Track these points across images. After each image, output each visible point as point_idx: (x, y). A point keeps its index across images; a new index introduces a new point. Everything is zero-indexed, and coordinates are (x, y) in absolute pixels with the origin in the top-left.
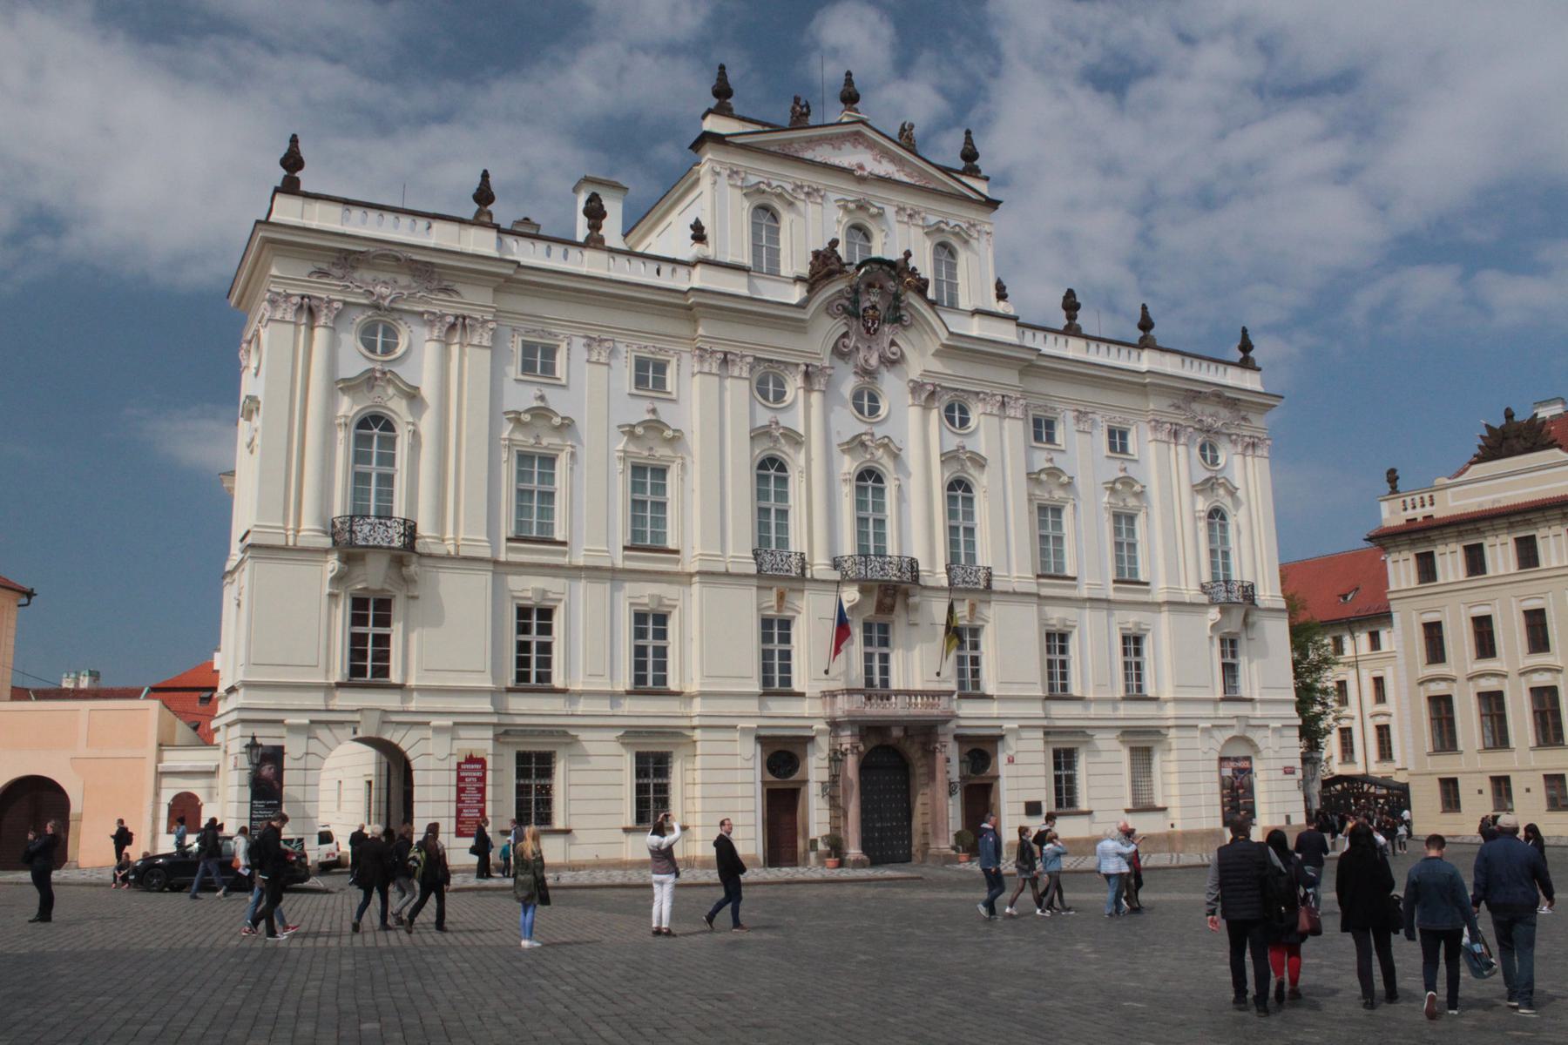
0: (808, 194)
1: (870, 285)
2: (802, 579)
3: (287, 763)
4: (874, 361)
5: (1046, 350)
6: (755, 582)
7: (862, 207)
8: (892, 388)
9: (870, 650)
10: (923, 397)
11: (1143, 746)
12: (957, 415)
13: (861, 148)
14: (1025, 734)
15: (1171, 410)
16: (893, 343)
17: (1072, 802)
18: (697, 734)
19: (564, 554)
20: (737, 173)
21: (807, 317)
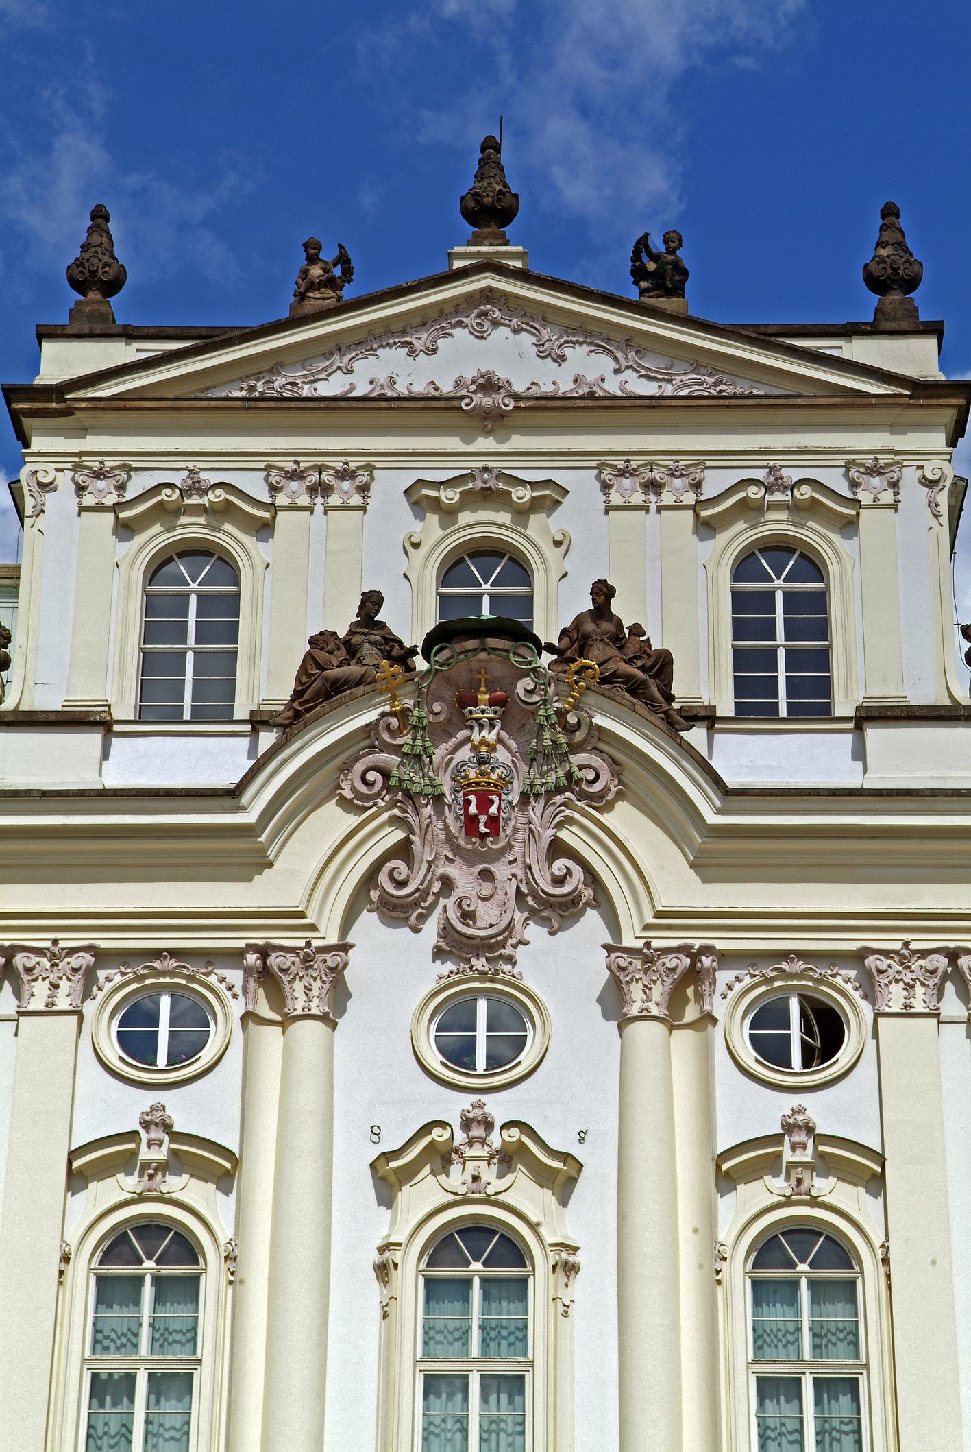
1: (466, 701)
10: (658, 992)
13: (504, 331)
16: (557, 849)
20: (100, 475)
21: (251, 817)
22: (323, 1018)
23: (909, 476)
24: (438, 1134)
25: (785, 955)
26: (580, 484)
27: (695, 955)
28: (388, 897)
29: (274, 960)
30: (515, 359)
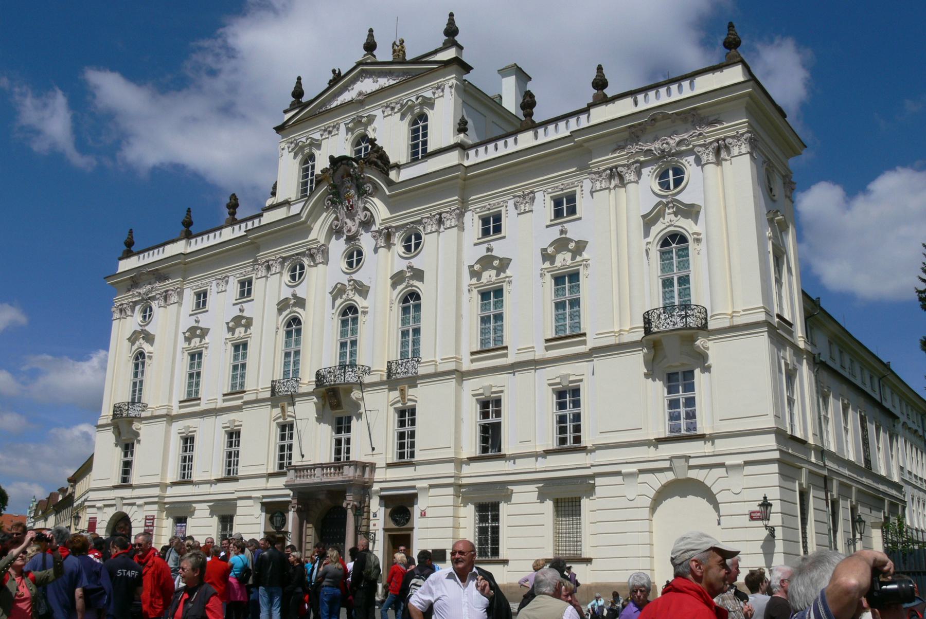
0: (330, 132)
1: (343, 177)
4: (354, 229)
7: (358, 122)
8: (366, 241)
11: (567, 498)
12: (413, 242)
14: (433, 491)
16: (366, 209)
17: (496, 552)
18: (239, 503)
19: (198, 405)
22: (322, 263)
23: (447, 87)
24: (339, 286)
26: (378, 113)
27: (387, 228)
28: (336, 232)
29: (313, 251)
30: (368, 85)
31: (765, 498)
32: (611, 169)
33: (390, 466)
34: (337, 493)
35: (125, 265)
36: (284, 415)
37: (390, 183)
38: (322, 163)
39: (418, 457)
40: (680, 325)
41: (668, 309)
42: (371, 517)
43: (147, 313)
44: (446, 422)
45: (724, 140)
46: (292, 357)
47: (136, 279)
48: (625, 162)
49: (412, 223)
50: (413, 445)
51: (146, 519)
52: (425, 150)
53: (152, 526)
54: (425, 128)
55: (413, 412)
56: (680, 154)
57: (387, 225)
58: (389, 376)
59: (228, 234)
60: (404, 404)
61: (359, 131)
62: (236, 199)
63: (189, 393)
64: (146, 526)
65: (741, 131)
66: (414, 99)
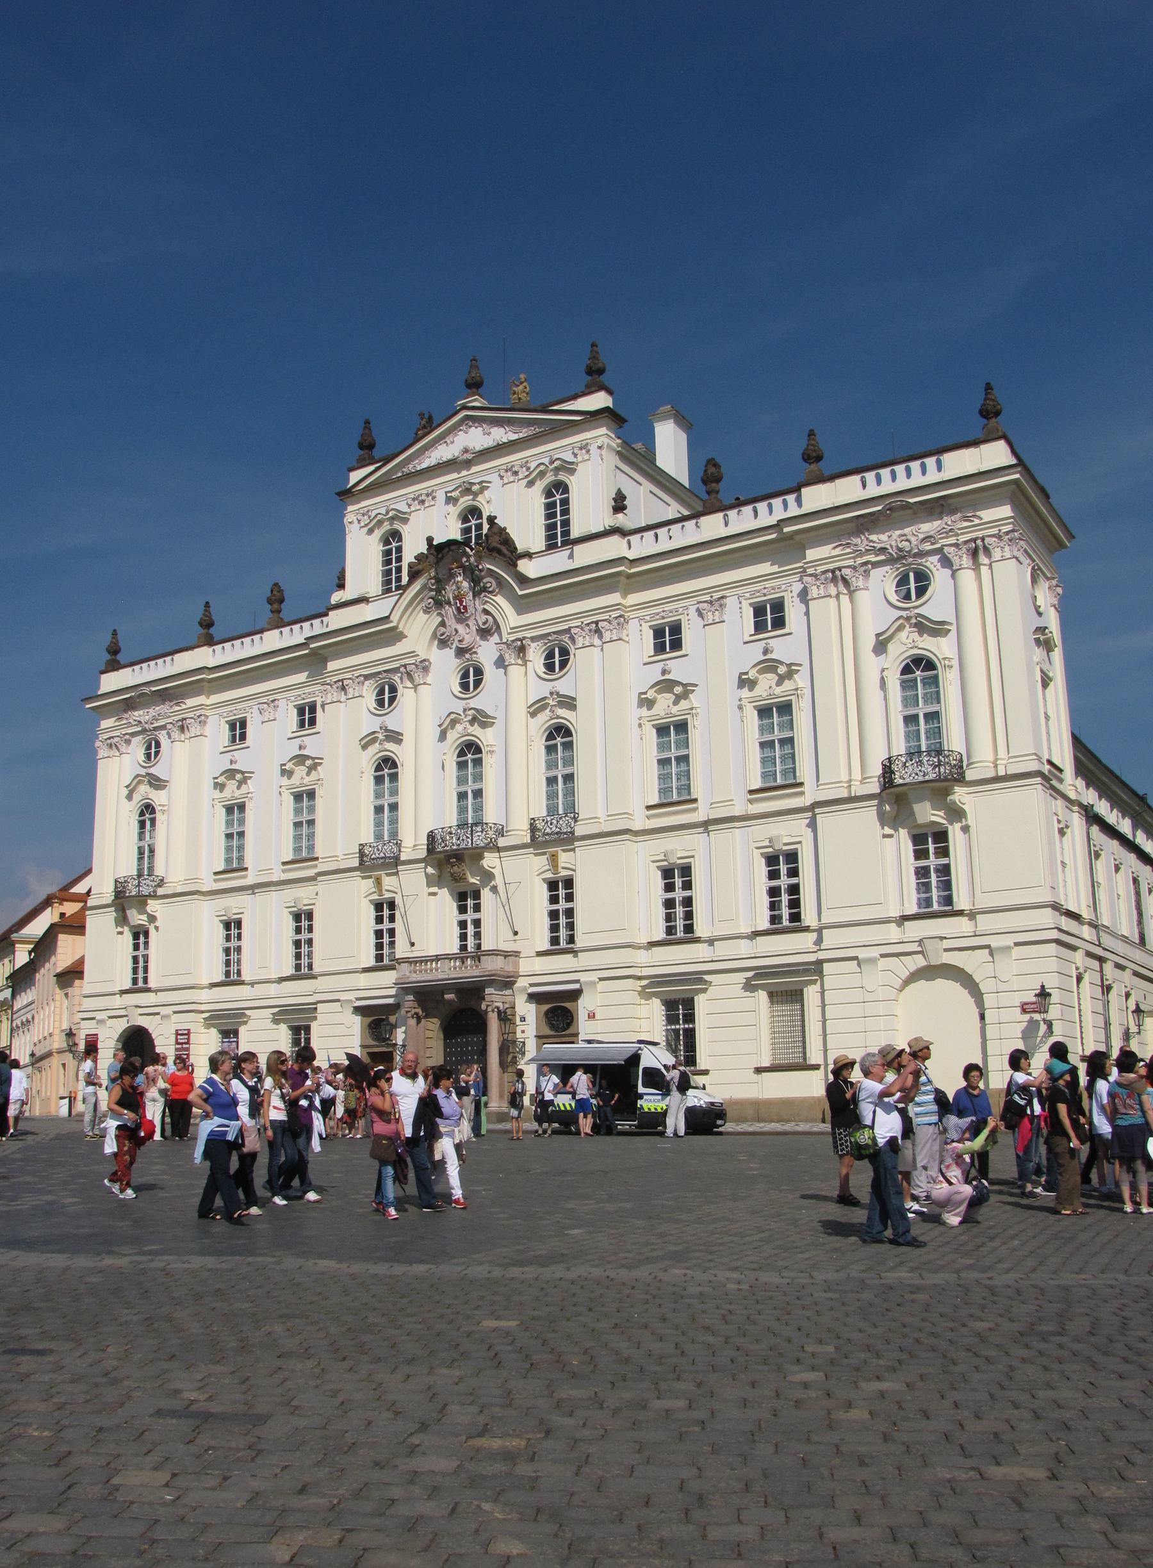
0: (423, 502)
2: (393, 863)
3: (100, 1045)
5: (631, 555)
6: (358, 873)
8: (486, 654)
9: (463, 917)
12: (558, 658)
15: (838, 551)
16: (486, 612)
19: (245, 877)
24: (453, 716)
25: (549, 634)
26: (494, 478)
27: (521, 640)
30: (476, 438)
31: (1043, 987)
32: (833, 571)
33: (540, 954)
34: (472, 992)
35: (111, 682)
36: (380, 890)
37: (523, 580)
38: (413, 547)
39: (580, 943)
40: (932, 776)
41: (913, 753)
42: (518, 1022)
43: (153, 750)
44: (620, 897)
45: (983, 539)
46: (387, 812)
47: (131, 701)
48: (850, 562)
49: (554, 633)
50: (571, 926)
51: (177, 1034)
52: (566, 533)
53: (188, 1043)
54: (565, 502)
55: (569, 883)
56: (922, 554)
57: (520, 635)
58: (533, 838)
59: (273, 640)
60: (556, 872)
61: (465, 501)
62: (280, 591)
63: (228, 860)
64: (177, 1043)
65: (1005, 529)
66: (546, 461)
